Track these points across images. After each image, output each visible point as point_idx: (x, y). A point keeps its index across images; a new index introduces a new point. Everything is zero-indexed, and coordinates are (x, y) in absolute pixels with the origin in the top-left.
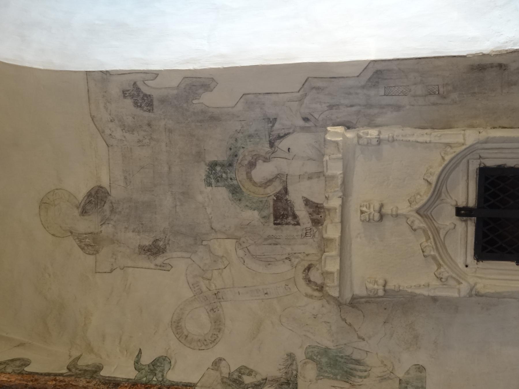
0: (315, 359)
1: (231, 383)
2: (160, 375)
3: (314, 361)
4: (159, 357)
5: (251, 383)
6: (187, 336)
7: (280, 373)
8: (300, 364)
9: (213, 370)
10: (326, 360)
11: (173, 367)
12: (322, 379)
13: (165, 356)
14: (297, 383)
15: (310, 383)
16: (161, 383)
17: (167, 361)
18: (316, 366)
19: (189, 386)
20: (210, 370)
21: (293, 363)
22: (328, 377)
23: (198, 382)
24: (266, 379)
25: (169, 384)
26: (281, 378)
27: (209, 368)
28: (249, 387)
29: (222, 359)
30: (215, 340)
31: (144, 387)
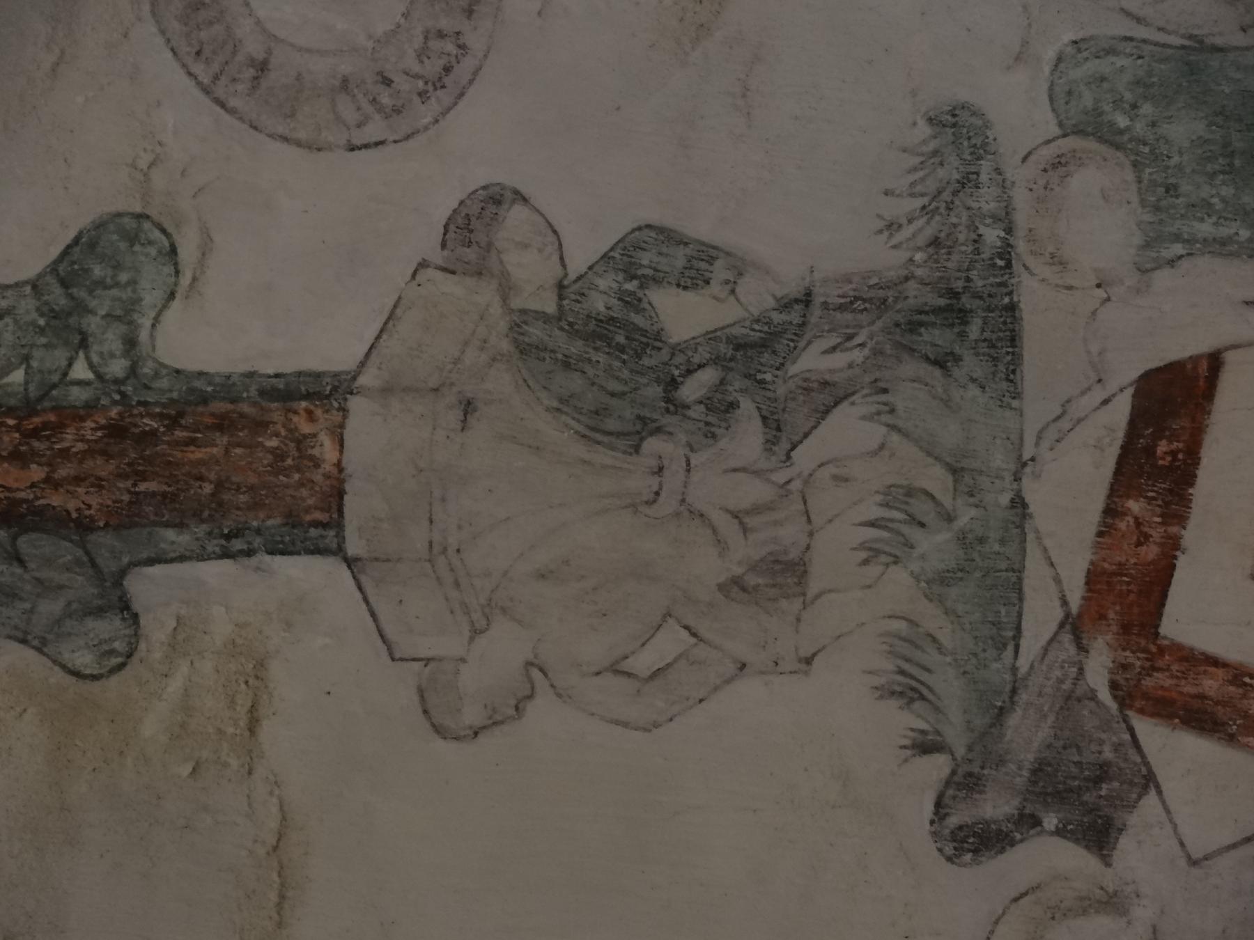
0: (1121, 132)
1: (576, 348)
2: (112, 340)
3: (1118, 147)
4: (100, 226)
5: (711, 336)
6: (262, 67)
7: (894, 247)
8: (1020, 175)
9: (453, 273)
10: (1200, 128)
11: (194, 279)
12: (1181, 257)
13: (138, 209)
14: (1012, 308)
15: (1101, 293)
16: (123, 394)
17: (150, 243)
18: (1130, 176)
19: (308, 396)
20: (430, 273)
21: (977, 174)
22: (1223, 242)
23: (362, 364)
24: (806, 299)
25: (175, 395)
26: (907, 279)
27: (423, 265)
28: (701, 366)
29: (508, 195)
30: (447, 69)
31: (17, 428)
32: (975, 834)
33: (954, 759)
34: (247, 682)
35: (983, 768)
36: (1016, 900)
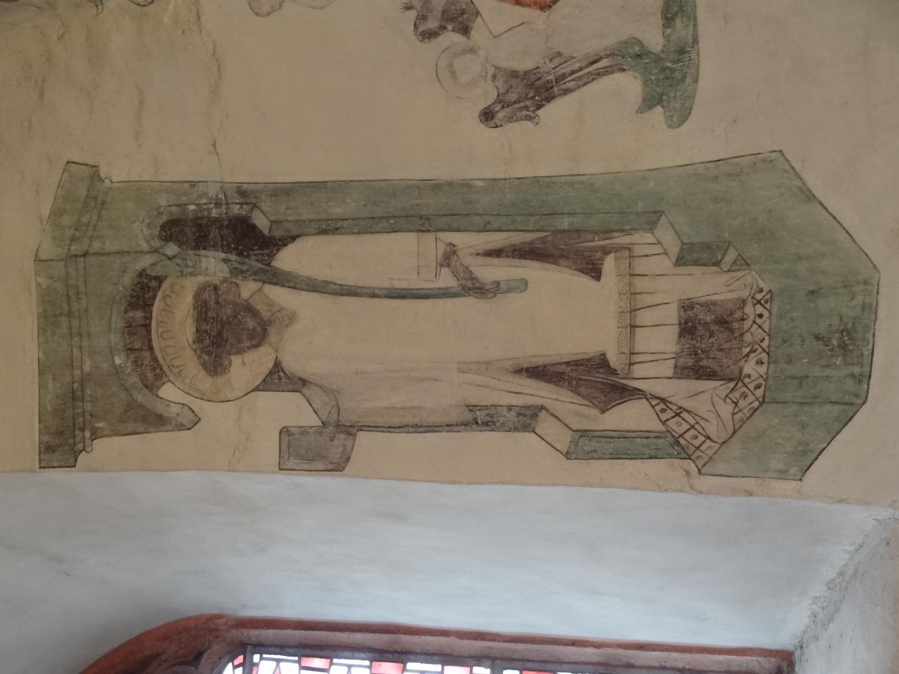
32: (428, 33)
33: (417, 11)
34: (194, 5)
35: (426, 13)
36: (443, 52)
